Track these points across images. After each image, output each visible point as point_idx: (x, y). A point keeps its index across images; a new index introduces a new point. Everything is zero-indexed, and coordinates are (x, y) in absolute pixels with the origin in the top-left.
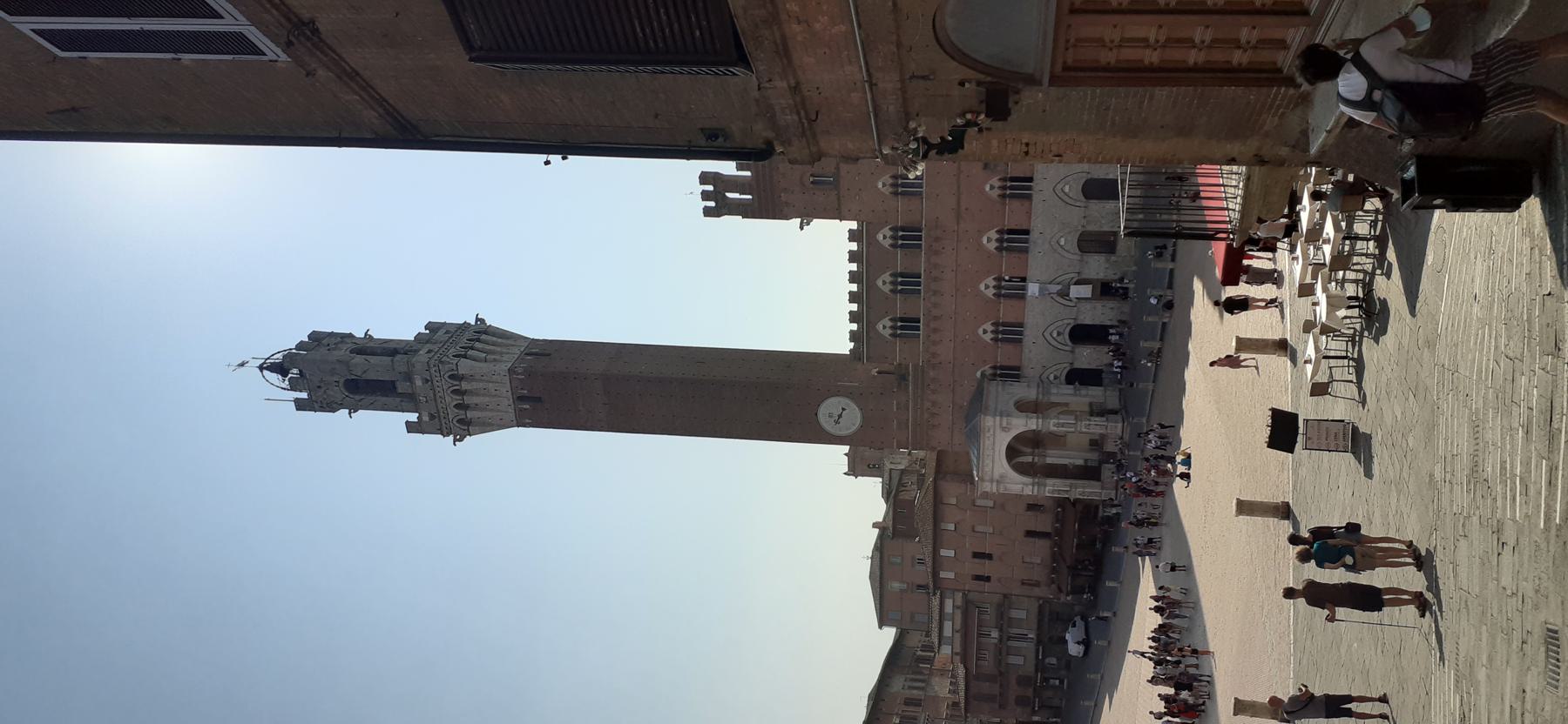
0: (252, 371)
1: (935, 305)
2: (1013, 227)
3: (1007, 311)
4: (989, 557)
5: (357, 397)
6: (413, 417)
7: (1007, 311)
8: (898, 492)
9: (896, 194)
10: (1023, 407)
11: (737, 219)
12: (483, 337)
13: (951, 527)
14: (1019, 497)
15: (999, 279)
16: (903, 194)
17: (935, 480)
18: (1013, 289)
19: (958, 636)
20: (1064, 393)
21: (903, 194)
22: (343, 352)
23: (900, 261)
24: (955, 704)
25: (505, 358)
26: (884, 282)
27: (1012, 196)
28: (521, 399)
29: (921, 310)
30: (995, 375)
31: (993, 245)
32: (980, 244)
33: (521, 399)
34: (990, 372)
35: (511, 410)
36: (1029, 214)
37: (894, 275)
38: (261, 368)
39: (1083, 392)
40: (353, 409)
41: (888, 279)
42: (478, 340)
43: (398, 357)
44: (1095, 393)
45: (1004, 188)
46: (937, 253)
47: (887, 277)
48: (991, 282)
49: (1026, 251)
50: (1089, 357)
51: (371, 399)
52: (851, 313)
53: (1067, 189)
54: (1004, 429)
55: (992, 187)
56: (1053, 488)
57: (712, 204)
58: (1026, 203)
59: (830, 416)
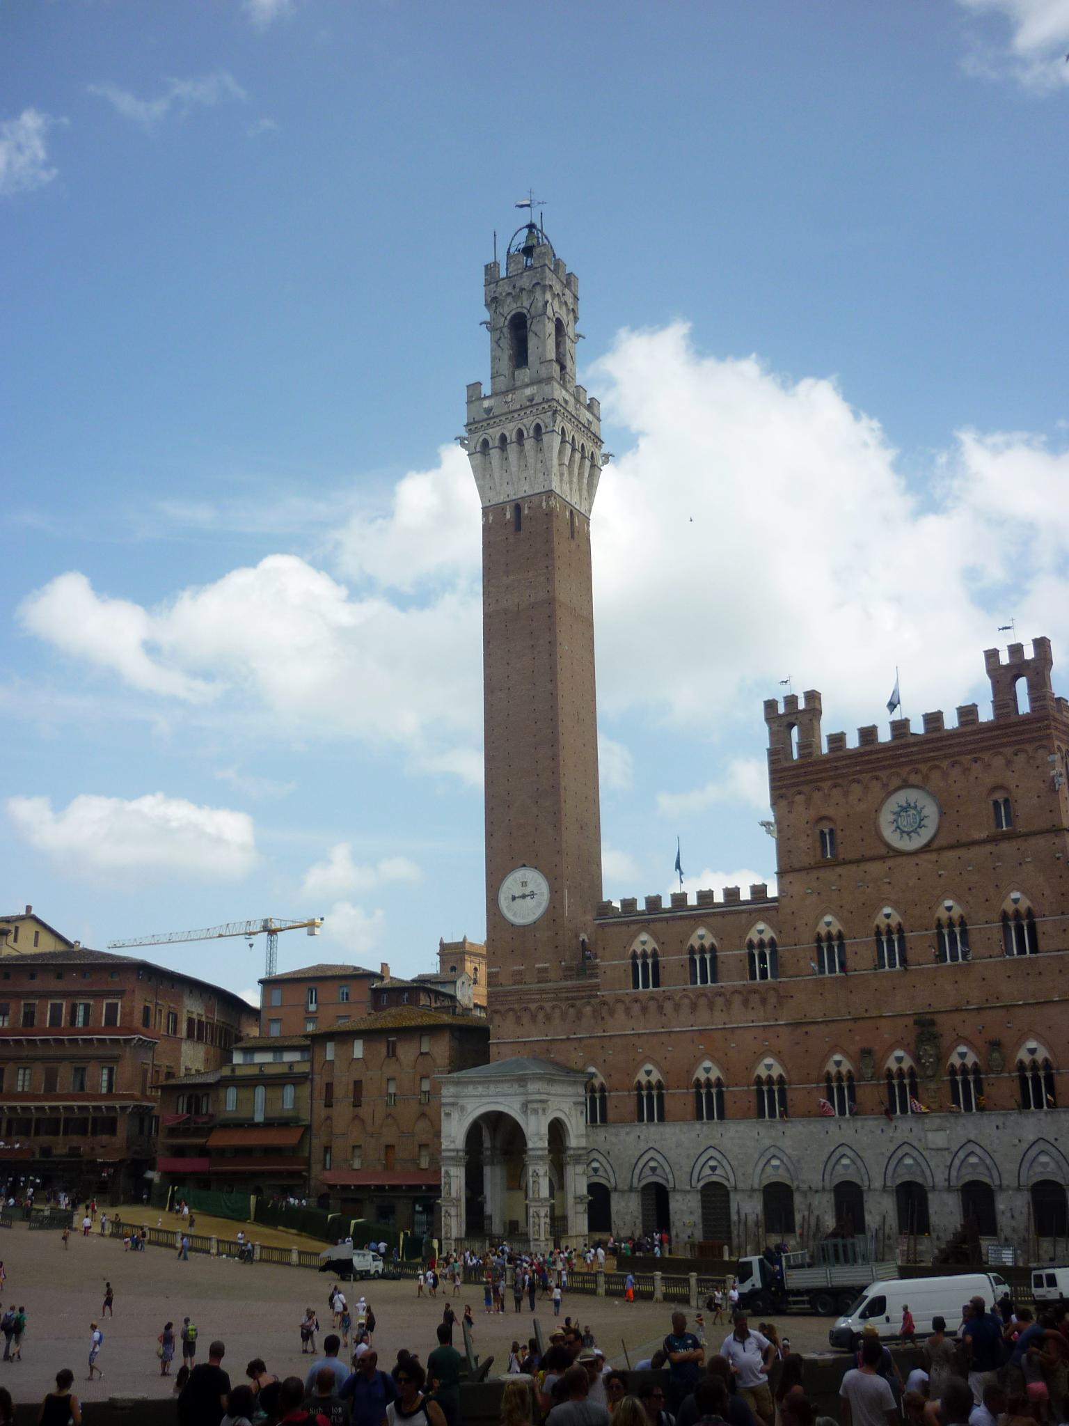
0: (525, 217)
1: (677, 1007)
2: (790, 1095)
3: (679, 1100)
4: (357, 1104)
5: (506, 330)
6: (486, 390)
7: (679, 1100)
8: (429, 992)
9: (819, 939)
10: (557, 1130)
11: (766, 743)
12: (588, 463)
14: (438, 1134)
16: (820, 949)
17: (449, 1027)
18: (710, 1103)
19: (255, 1071)
20: (577, 1183)
21: (820, 949)
22: (555, 309)
23: (732, 955)
24: (170, 1075)
25: (566, 487)
26: (702, 936)
28: (518, 509)
30: (593, 1090)
31: (762, 1072)
33: (518, 509)
34: (596, 1082)
35: (502, 498)
37: (713, 949)
38: (531, 226)
39: (582, 1208)
40: (491, 327)
41: (707, 944)
42: (583, 457)
43: (556, 367)
44: (579, 1223)
45: (839, 1077)
46: (745, 1003)
47: (708, 941)
48: (715, 1074)
49: (761, 1114)
50: (627, 1211)
51: (506, 343)
52: (659, 898)
53: (845, 1161)
54: (525, 1105)
55: (838, 1063)
56: (455, 1180)
57: (781, 709)
59: (524, 884)
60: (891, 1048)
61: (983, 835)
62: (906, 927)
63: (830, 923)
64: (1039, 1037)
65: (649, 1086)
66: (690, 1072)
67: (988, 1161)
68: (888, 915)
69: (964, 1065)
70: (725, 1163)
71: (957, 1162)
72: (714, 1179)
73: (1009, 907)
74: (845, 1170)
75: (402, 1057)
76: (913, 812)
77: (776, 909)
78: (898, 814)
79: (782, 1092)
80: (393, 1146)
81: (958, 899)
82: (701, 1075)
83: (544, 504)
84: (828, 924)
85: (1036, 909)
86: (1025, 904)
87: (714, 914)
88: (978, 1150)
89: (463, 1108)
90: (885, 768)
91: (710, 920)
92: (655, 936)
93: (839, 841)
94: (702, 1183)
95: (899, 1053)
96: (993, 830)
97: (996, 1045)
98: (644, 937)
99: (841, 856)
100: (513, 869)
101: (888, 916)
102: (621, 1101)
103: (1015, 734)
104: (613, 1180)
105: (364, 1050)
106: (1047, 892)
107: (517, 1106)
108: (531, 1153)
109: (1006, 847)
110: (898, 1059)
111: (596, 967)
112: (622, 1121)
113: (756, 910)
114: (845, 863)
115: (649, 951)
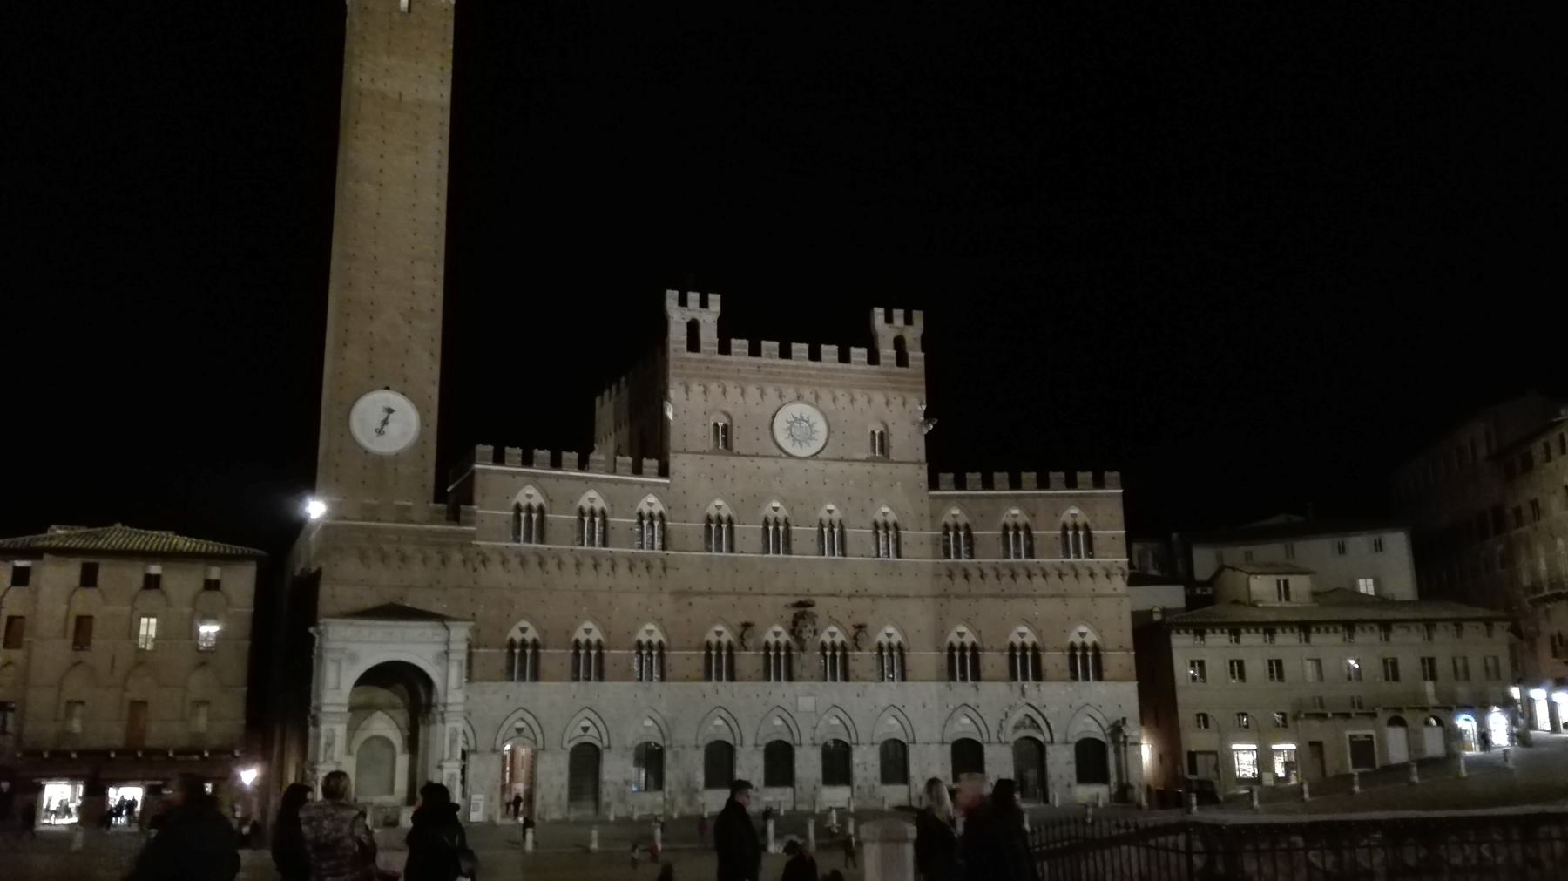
2: (668, 661)
3: (555, 658)
9: (709, 520)
15: (599, 646)
18: (589, 663)
21: (708, 528)
27: (708, 656)
36: (687, 679)
45: (719, 646)
47: (599, 504)
48: (596, 635)
55: (719, 633)
58: (701, 674)
61: (864, 456)
62: (791, 521)
63: (720, 506)
64: (896, 624)
65: (524, 644)
66: (569, 633)
67: (849, 723)
68: (775, 507)
70: (599, 724)
71: (822, 723)
72: (586, 739)
73: (880, 520)
74: (717, 728)
78: (791, 423)
80: (144, 703)
81: (839, 505)
82: (581, 636)
84: (718, 507)
85: (900, 523)
86: (892, 518)
87: (608, 480)
88: (841, 714)
89: (353, 658)
91: (604, 485)
94: (573, 744)
95: (778, 628)
96: (871, 454)
97: (860, 627)
98: (530, 490)
99: (736, 450)
100: (371, 390)
101: (776, 509)
104: (472, 743)
108: (450, 708)
109: (881, 468)
110: (776, 633)
111: (473, 513)
112: (490, 679)
113: (649, 484)
114: (738, 454)
115: (535, 505)
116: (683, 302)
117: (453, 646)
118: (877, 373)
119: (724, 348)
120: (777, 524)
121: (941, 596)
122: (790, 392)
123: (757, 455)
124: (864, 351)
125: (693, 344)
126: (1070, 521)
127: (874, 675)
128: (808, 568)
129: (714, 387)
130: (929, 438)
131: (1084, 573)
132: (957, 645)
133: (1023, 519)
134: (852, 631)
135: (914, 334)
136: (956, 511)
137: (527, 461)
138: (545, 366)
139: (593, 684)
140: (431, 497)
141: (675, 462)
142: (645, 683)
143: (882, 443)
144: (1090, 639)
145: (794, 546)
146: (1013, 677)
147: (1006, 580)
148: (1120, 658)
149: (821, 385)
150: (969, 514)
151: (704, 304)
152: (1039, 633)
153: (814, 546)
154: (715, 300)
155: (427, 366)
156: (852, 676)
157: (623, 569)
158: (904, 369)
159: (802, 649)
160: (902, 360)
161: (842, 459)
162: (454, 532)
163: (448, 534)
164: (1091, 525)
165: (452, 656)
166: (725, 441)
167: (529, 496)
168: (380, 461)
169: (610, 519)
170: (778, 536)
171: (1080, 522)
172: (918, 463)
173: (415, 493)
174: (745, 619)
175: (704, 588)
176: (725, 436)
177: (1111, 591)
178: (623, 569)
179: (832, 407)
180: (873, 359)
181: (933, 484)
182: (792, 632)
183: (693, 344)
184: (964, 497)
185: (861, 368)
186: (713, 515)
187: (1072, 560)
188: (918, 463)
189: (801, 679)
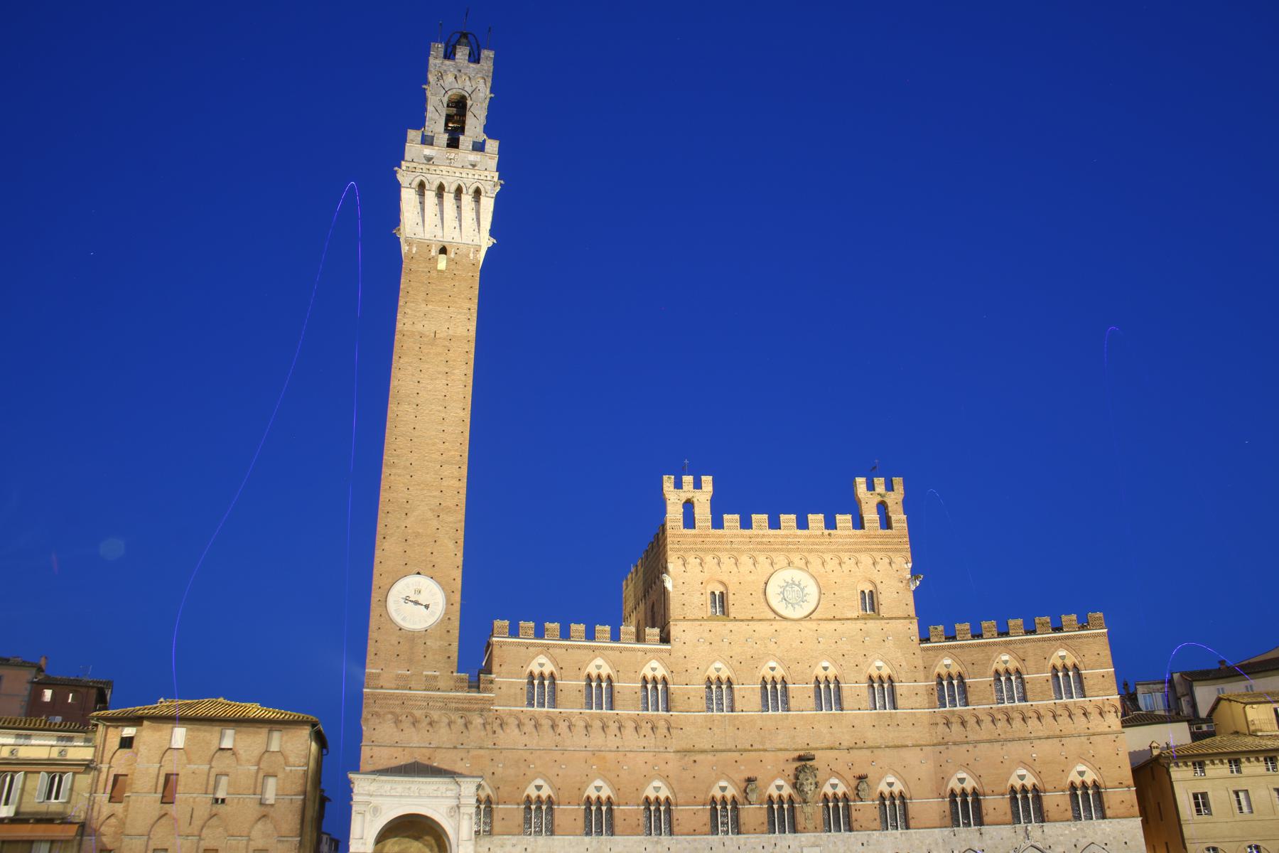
2: (675, 815)
3: (569, 813)
7: (569, 813)
13: (227, 743)
15: (609, 802)
29: (572, 707)
32: (652, 779)
36: (694, 833)
37: (609, 678)
47: (605, 671)
55: (723, 789)
60: (774, 779)
61: (855, 615)
62: (788, 680)
64: (896, 774)
68: (771, 668)
69: (835, 794)
73: (875, 674)
75: (241, 752)
76: (796, 588)
77: (667, 651)
78: (784, 588)
79: (668, 811)
81: (834, 661)
83: (471, 255)
84: (718, 670)
85: (895, 677)
86: (885, 672)
89: (376, 810)
90: (775, 550)
92: (554, 661)
93: (731, 602)
98: (542, 659)
99: (732, 616)
101: (773, 669)
102: (509, 811)
103: (881, 543)
105: (188, 740)
106: (904, 664)
107: (444, 810)
109: (872, 625)
110: (779, 787)
111: (491, 682)
113: (651, 651)
114: (735, 619)
116: (678, 485)
117: (463, 801)
118: (862, 536)
119: (717, 523)
120: (774, 682)
121: (939, 744)
122: (780, 559)
123: (752, 619)
124: (849, 517)
125: (689, 521)
126: (1059, 664)
127: (877, 823)
128: (804, 724)
129: (708, 559)
130: (917, 594)
131: (1079, 712)
132: (958, 791)
133: (1012, 665)
134: (854, 783)
135: (895, 499)
136: (948, 661)
137: (540, 633)
138: (563, 549)
139: (604, 837)
140: (455, 668)
141: (675, 630)
142: (654, 838)
143: (870, 601)
144: (1089, 778)
145: (792, 703)
146: (1016, 819)
147: (1002, 724)
148: (1122, 795)
149: (811, 551)
150: (962, 663)
151: (698, 485)
152: (1038, 774)
153: (812, 702)
154: (707, 481)
155: (452, 553)
156: (855, 825)
157: (629, 730)
158: (888, 532)
159: (805, 802)
160: (886, 523)
161: (834, 619)
162: (476, 699)
163: (470, 700)
164: (1081, 666)
165: (462, 810)
166: (722, 606)
167: (541, 665)
168: (412, 638)
169: (615, 684)
170: (775, 694)
171: (1069, 663)
172: (908, 617)
173: (441, 665)
174: (747, 775)
175: (708, 747)
176: (721, 601)
177: (1107, 730)
178: (629, 730)
179: (822, 570)
180: (859, 523)
181: (925, 638)
182: (794, 786)
183: (689, 521)
184: (955, 647)
185: (847, 532)
186: (713, 677)
187: (1065, 700)
188: (908, 617)
189: (805, 830)
